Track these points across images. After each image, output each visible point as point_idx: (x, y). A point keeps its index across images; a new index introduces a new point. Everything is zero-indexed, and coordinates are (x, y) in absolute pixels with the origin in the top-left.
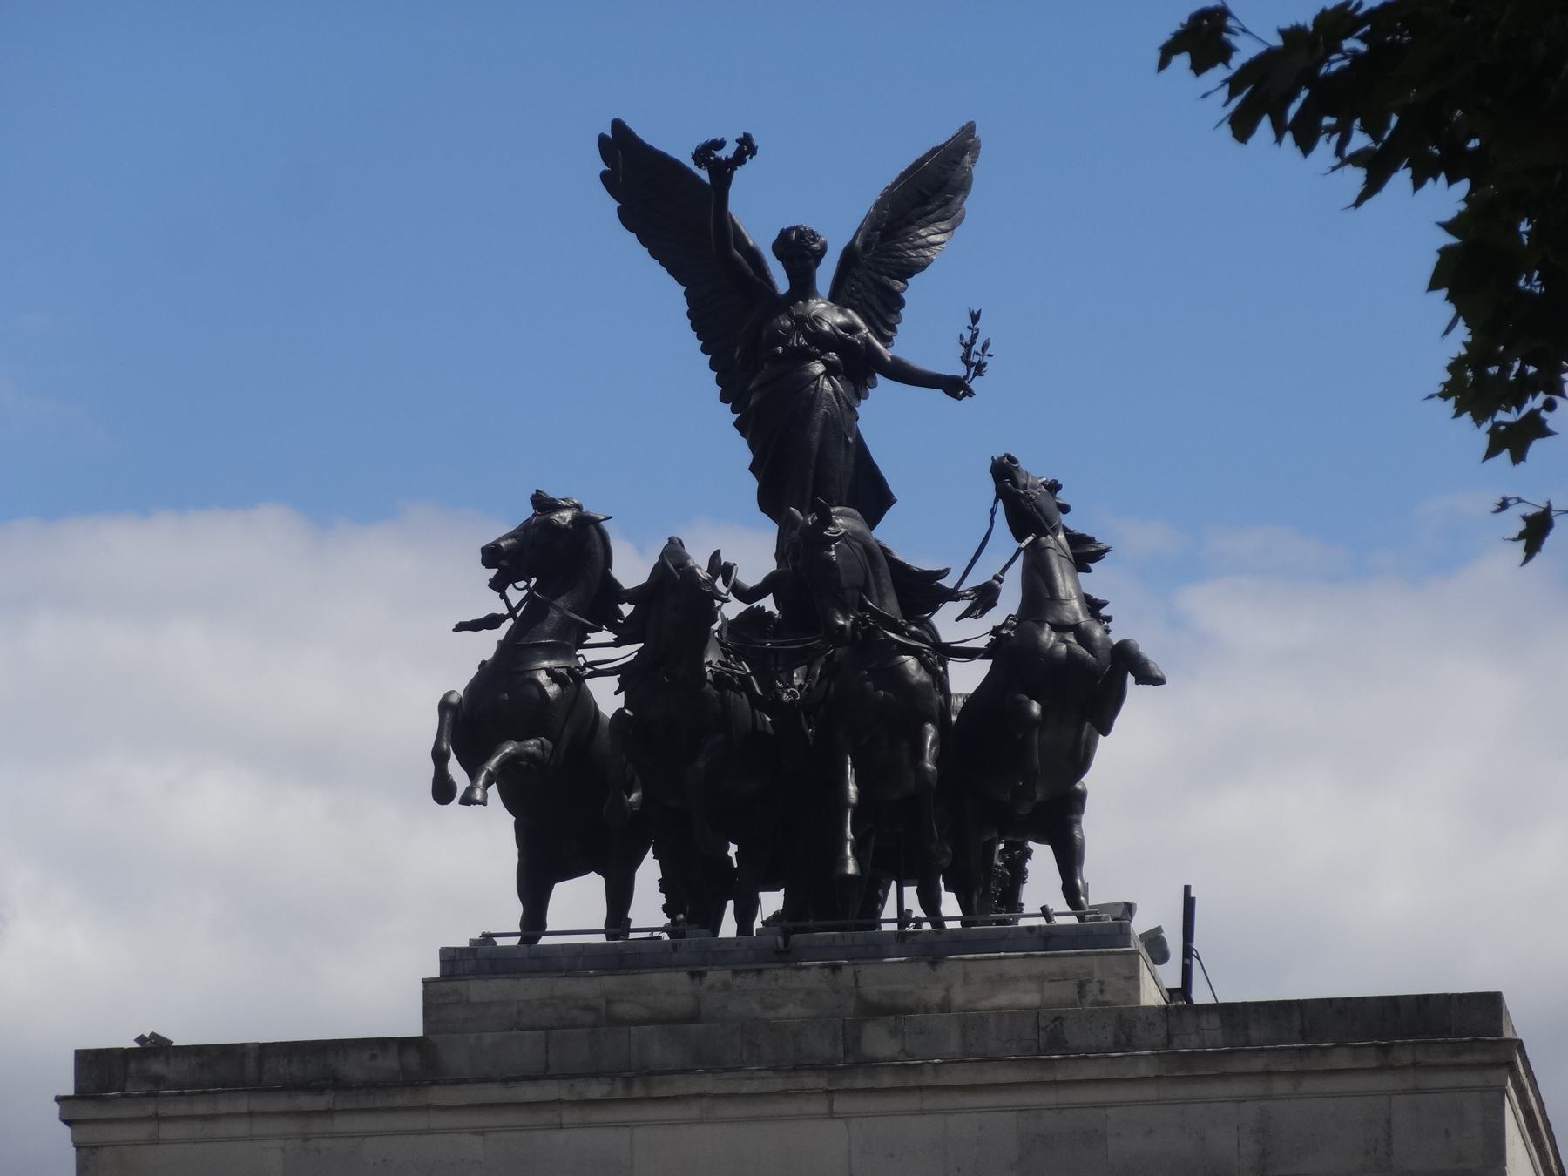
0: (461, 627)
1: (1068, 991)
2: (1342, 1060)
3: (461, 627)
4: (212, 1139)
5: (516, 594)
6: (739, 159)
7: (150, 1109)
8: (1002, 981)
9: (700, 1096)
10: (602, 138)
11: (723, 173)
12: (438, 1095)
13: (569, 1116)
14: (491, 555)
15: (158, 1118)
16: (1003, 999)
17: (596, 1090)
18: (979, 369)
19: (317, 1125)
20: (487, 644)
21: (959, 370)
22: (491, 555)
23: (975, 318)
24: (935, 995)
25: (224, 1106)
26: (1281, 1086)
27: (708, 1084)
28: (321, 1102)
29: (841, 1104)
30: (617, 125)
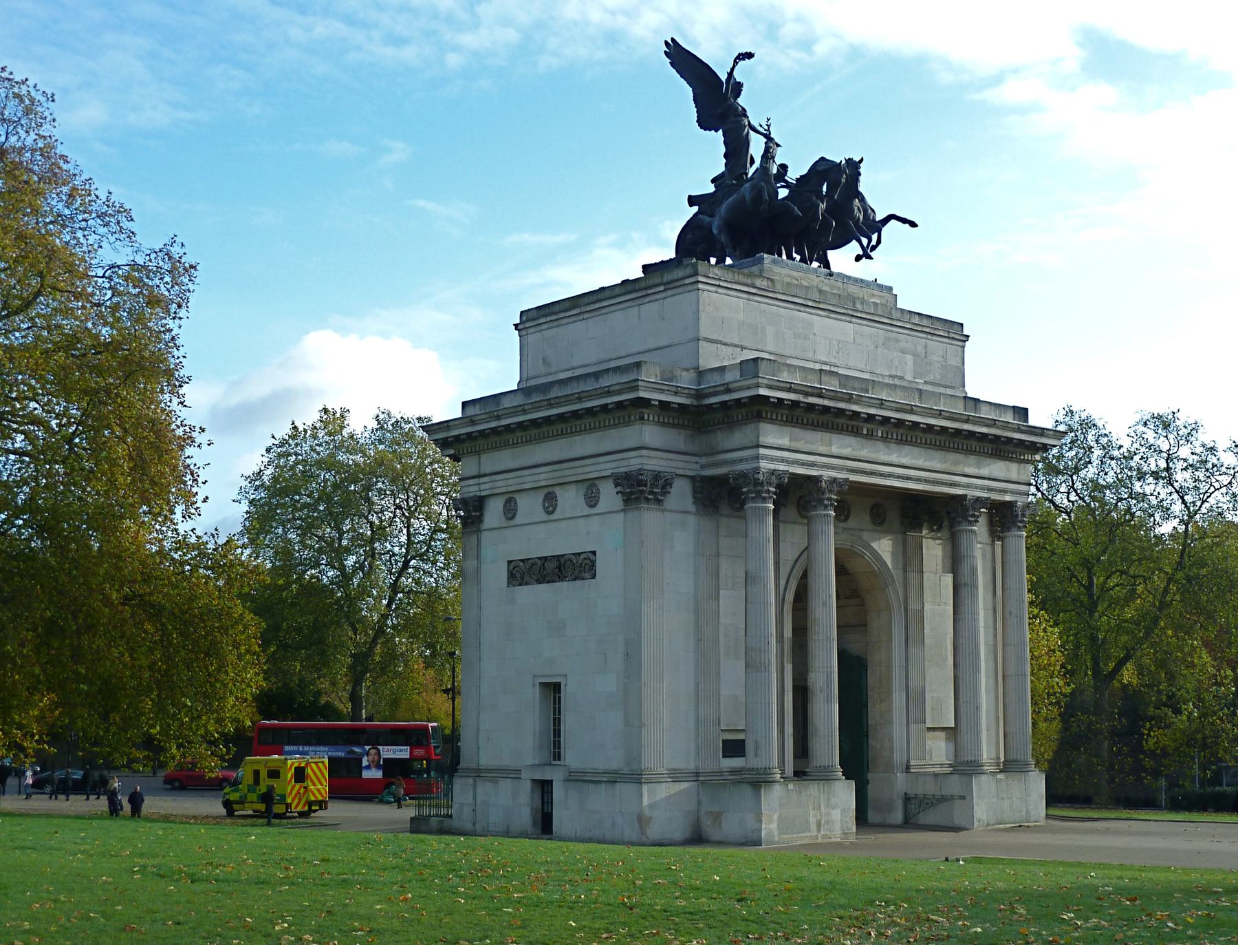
1: (884, 302)
4: (729, 295)
7: (717, 283)
8: (873, 295)
9: (829, 310)
10: (666, 43)
11: (735, 63)
13: (802, 309)
15: (719, 286)
16: (873, 300)
18: (770, 134)
19: (751, 297)
23: (768, 120)
24: (861, 296)
26: (930, 337)
28: (754, 291)
29: (854, 320)
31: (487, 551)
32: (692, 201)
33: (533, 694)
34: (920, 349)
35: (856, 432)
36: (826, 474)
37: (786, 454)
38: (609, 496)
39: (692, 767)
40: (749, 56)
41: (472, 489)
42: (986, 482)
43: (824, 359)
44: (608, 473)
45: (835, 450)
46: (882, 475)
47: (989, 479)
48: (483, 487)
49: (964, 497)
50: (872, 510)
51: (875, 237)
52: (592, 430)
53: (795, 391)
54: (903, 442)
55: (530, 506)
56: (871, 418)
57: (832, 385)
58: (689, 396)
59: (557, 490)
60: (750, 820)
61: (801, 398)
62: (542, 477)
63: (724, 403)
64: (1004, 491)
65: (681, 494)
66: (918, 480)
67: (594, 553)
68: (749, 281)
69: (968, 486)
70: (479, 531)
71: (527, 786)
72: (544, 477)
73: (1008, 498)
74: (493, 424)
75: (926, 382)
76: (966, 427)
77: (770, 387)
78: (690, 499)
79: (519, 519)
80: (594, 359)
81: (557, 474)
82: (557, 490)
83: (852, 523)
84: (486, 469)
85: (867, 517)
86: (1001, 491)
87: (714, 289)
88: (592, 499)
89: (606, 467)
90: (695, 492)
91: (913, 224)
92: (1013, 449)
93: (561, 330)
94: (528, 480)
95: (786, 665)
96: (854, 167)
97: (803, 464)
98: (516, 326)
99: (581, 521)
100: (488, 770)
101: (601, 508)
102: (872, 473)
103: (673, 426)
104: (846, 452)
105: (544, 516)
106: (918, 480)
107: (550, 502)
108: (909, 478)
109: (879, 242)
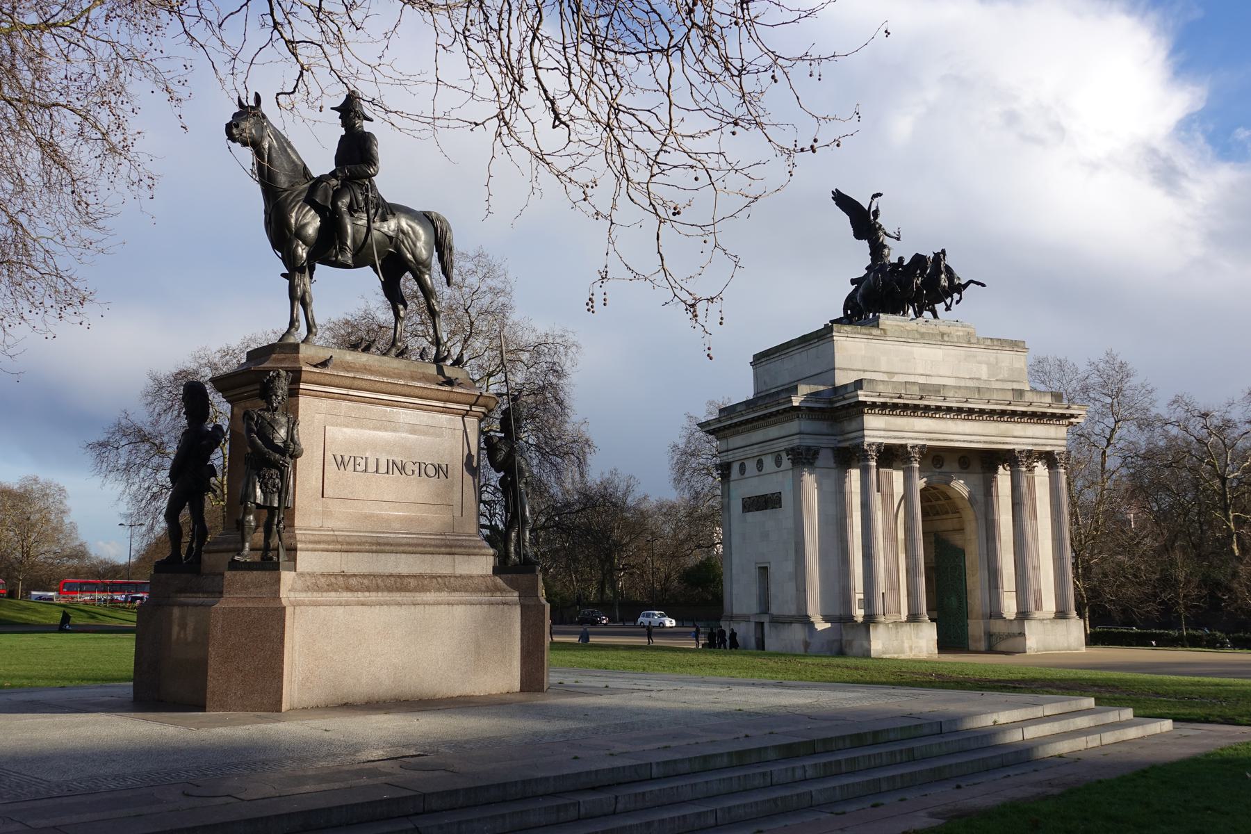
2: (1007, 349)
8: (958, 331)
13: (905, 344)
16: (958, 333)
25: (857, 336)
28: (871, 337)
30: (836, 190)
31: (733, 494)
32: (853, 281)
33: (754, 573)
34: (992, 360)
36: (910, 443)
37: (882, 433)
38: (786, 463)
39: (838, 614)
40: (879, 195)
41: (725, 458)
42: (1031, 441)
43: (922, 373)
44: (783, 448)
45: (917, 428)
46: (951, 441)
48: (730, 457)
49: (1014, 450)
50: (960, 460)
51: (956, 296)
52: (775, 424)
53: (884, 397)
55: (751, 466)
56: (938, 409)
57: (916, 390)
58: (824, 403)
59: (763, 458)
60: (865, 643)
61: (888, 400)
62: (755, 450)
63: (843, 406)
65: (825, 458)
66: (980, 442)
67: (780, 493)
69: (1017, 444)
70: (729, 481)
71: (753, 625)
72: (755, 450)
73: (1048, 449)
74: (729, 422)
75: (997, 380)
78: (832, 461)
79: (747, 475)
80: (787, 382)
81: (761, 449)
82: (763, 458)
83: (945, 469)
84: (731, 447)
85: (956, 466)
86: (1043, 445)
88: (778, 462)
89: (784, 444)
90: (835, 457)
91: (983, 285)
93: (772, 365)
94: (750, 452)
95: (900, 555)
96: (939, 257)
97: (895, 438)
98: (751, 363)
99: (774, 475)
100: (738, 616)
101: (782, 467)
102: (944, 440)
103: (819, 419)
104: (924, 428)
105: (757, 473)
106: (980, 442)
107: (760, 464)
108: (971, 442)
109: (961, 298)
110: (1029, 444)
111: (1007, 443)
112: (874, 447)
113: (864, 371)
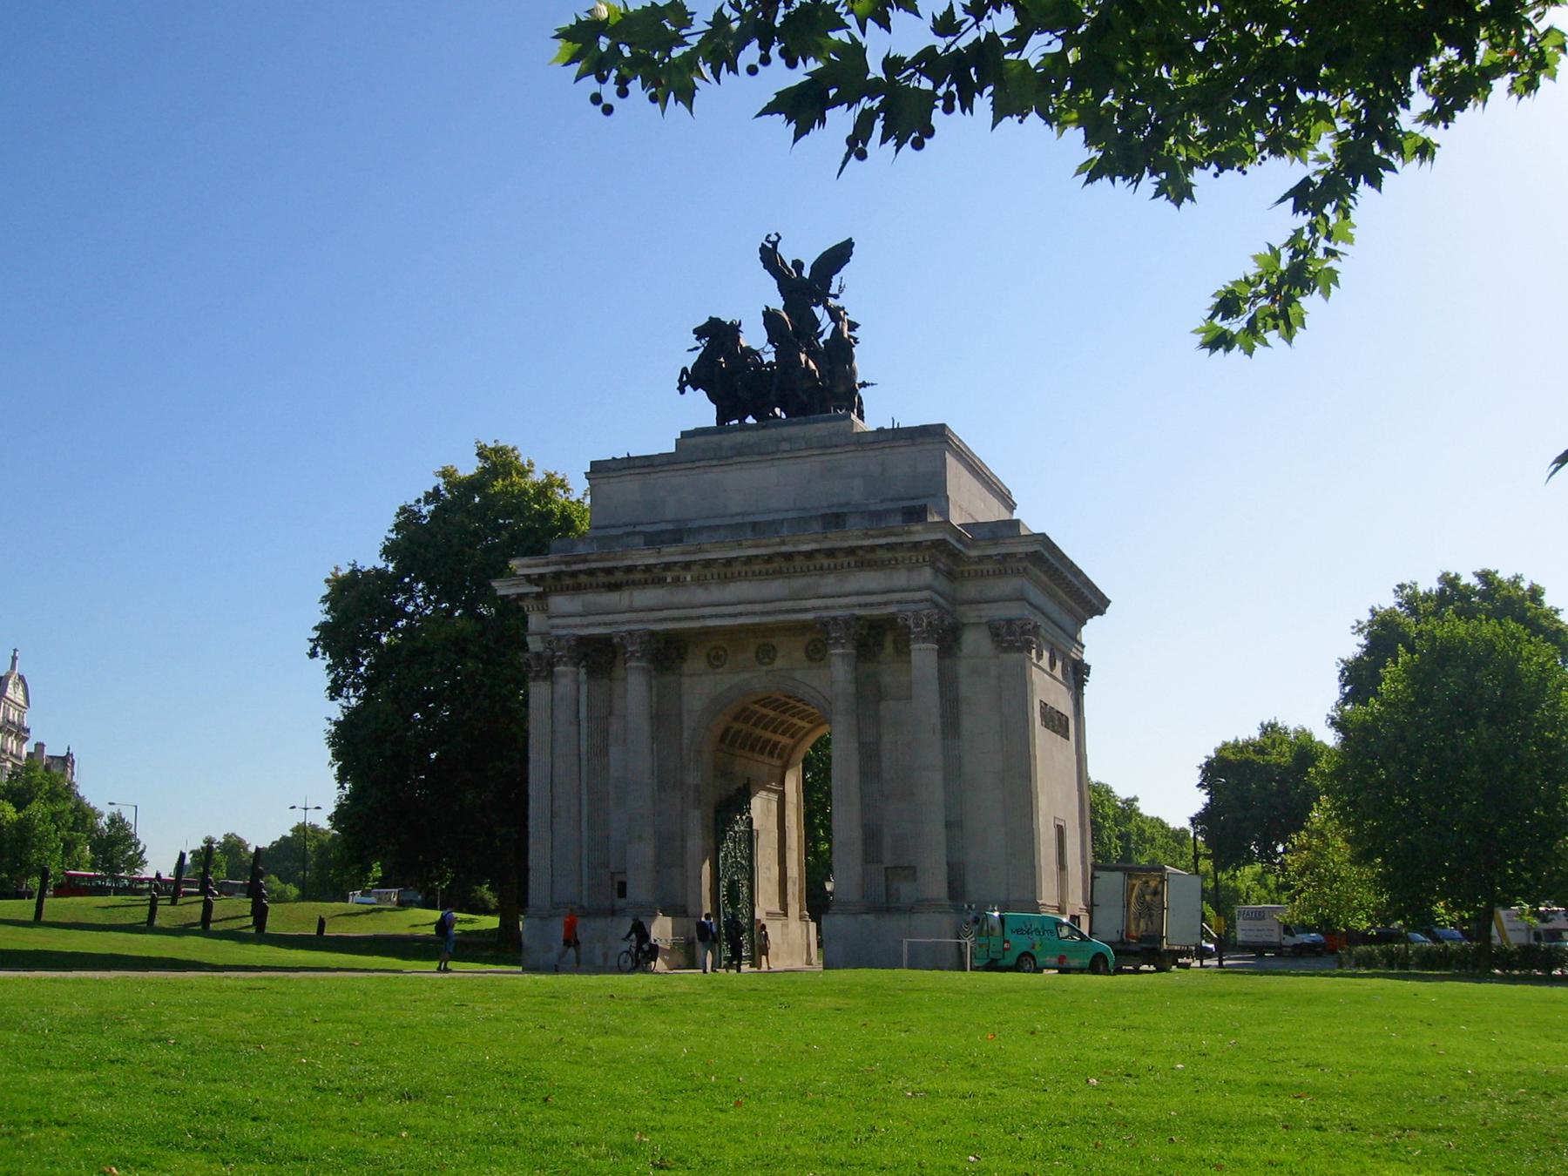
0: (689, 350)
2: (902, 443)
3: (689, 350)
5: (703, 342)
6: (778, 241)
11: (775, 244)
12: (676, 467)
14: (695, 331)
17: (715, 463)
19: (648, 476)
20: (695, 356)
21: (837, 292)
22: (695, 331)
27: (741, 459)
29: (776, 463)
35: (660, 582)
37: (578, 620)
40: (769, 235)
42: (854, 600)
47: (858, 594)
54: (724, 579)
61: (563, 568)
64: (886, 604)
66: (754, 614)
68: (647, 463)
69: (827, 608)
73: (892, 609)
75: (882, 501)
76: (784, 549)
77: (529, 566)
86: (880, 604)
87: (605, 481)
92: (889, 555)
97: (599, 624)
106: (754, 614)
108: (735, 615)
110: (848, 607)
111: (806, 610)
112: (563, 642)
113: (635, 525)
